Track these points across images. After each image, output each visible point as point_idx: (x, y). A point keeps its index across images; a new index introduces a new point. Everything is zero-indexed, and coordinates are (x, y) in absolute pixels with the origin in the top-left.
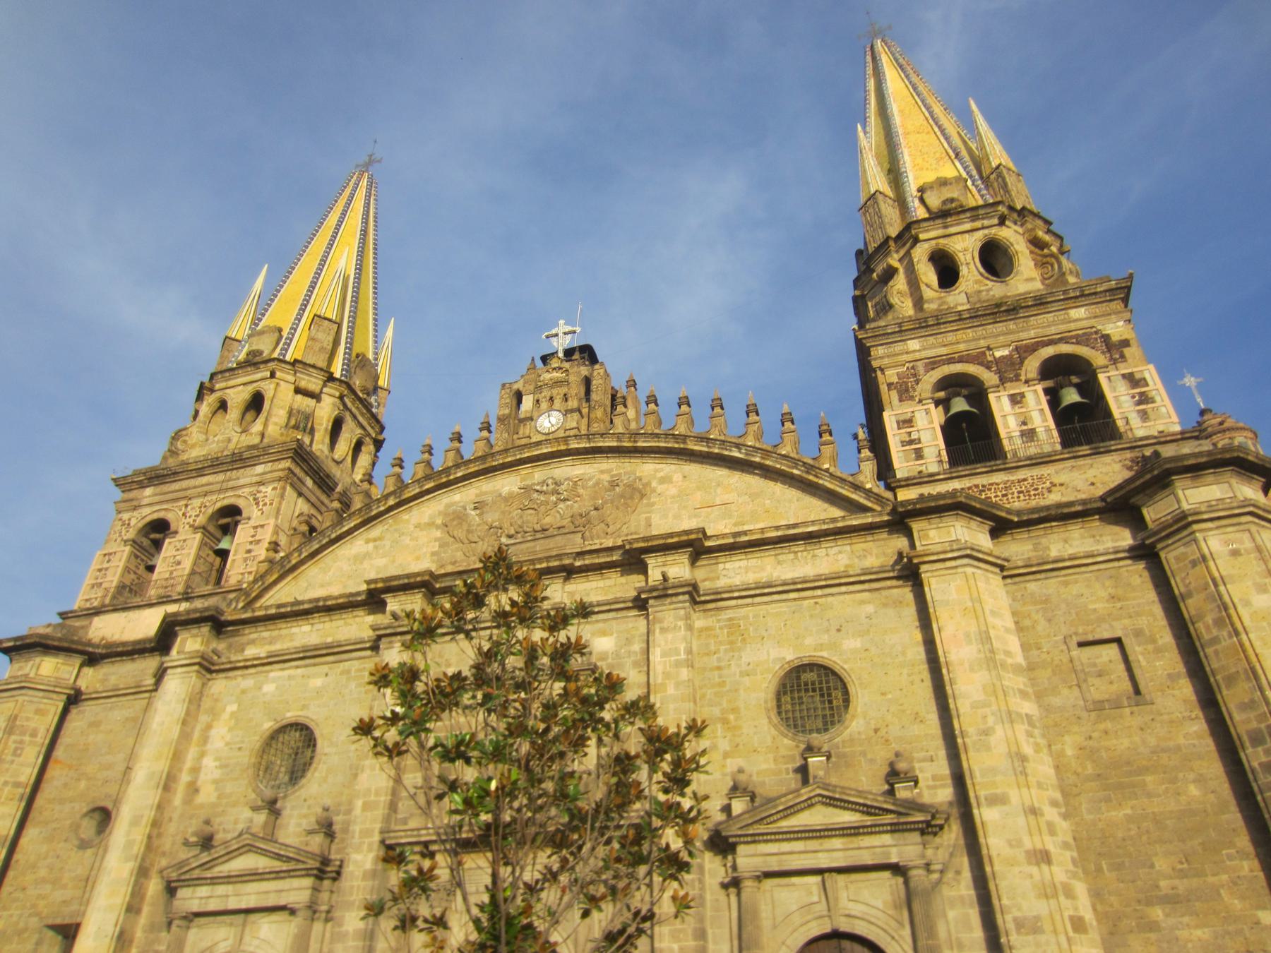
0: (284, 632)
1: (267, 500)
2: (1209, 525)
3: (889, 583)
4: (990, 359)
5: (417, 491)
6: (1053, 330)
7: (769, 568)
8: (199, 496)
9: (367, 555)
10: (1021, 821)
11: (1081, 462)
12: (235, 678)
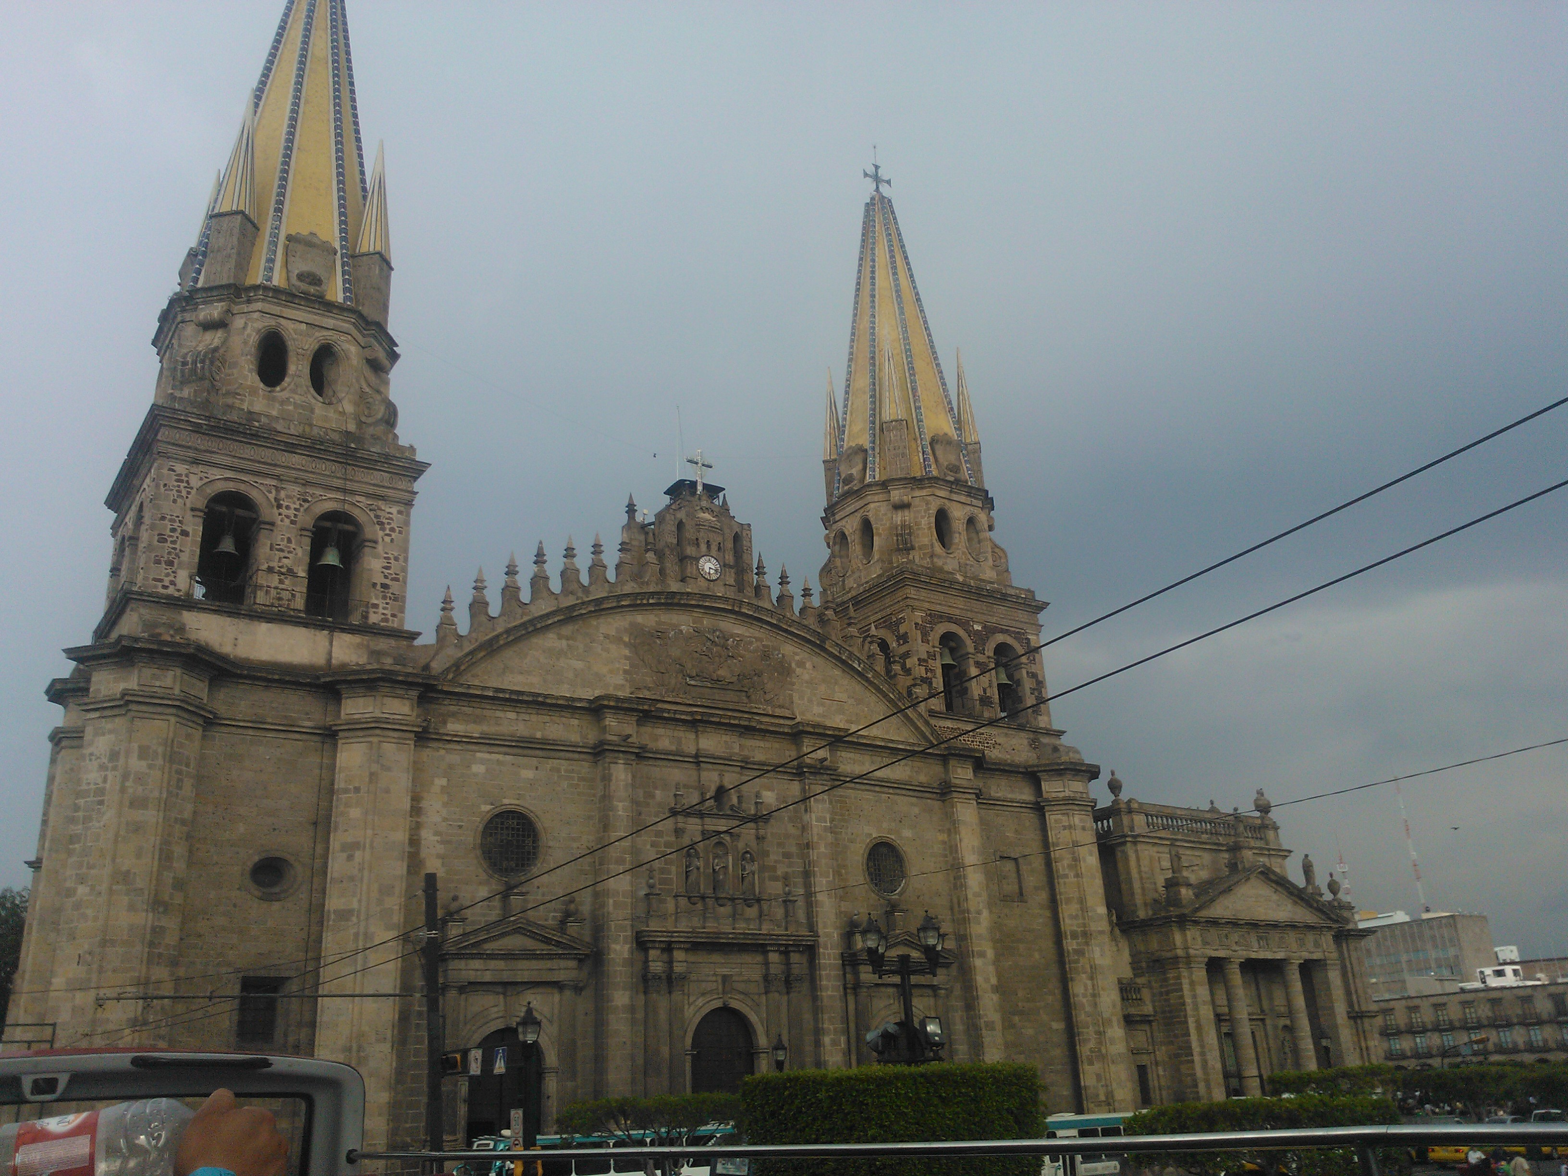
1: (394, 525)
2: (1076, 808)
3: (927, 795)
5: (614, 604)
6: (1005, 622)
8: (296, 481)
11: (1011, 732)
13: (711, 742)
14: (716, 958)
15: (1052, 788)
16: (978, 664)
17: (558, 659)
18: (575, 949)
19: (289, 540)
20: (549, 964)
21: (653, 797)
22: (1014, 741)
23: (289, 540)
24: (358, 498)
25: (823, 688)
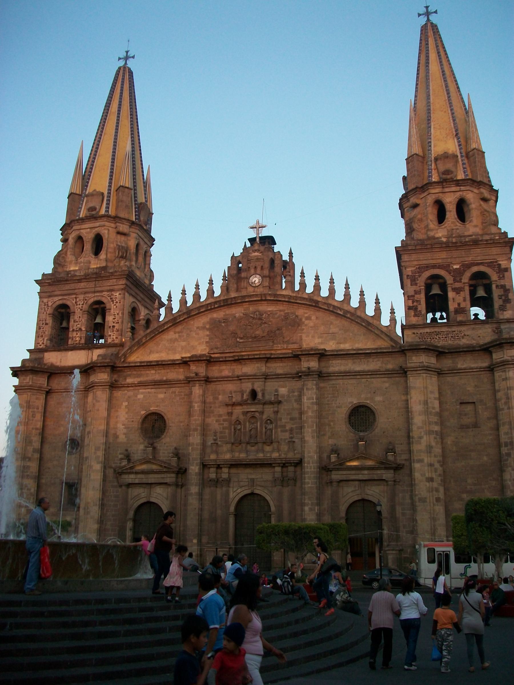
0: (142, 372)
1: (117, 300)
3: (395, 375)
4: (451, 269)
5: (197, 312)
6: (479, 258)
7: (350, 365)
8: (81, 293)
9: (176, 340)
10: (426, 468)
12: (124, 390)
13: (248, 369)
14: (248, 470)
15: (497, 356)
16: (454, 290)
17: (174, 343)
18: (171, 469)
19: (80, 317)
20: (163, 475)
21: (218, 399)
22: (480, 331)
23: (80, 317)
24: (104, 293)
25: (322, 328)
